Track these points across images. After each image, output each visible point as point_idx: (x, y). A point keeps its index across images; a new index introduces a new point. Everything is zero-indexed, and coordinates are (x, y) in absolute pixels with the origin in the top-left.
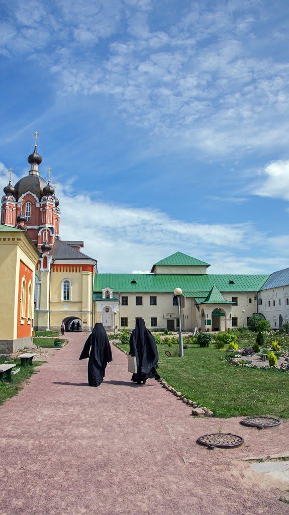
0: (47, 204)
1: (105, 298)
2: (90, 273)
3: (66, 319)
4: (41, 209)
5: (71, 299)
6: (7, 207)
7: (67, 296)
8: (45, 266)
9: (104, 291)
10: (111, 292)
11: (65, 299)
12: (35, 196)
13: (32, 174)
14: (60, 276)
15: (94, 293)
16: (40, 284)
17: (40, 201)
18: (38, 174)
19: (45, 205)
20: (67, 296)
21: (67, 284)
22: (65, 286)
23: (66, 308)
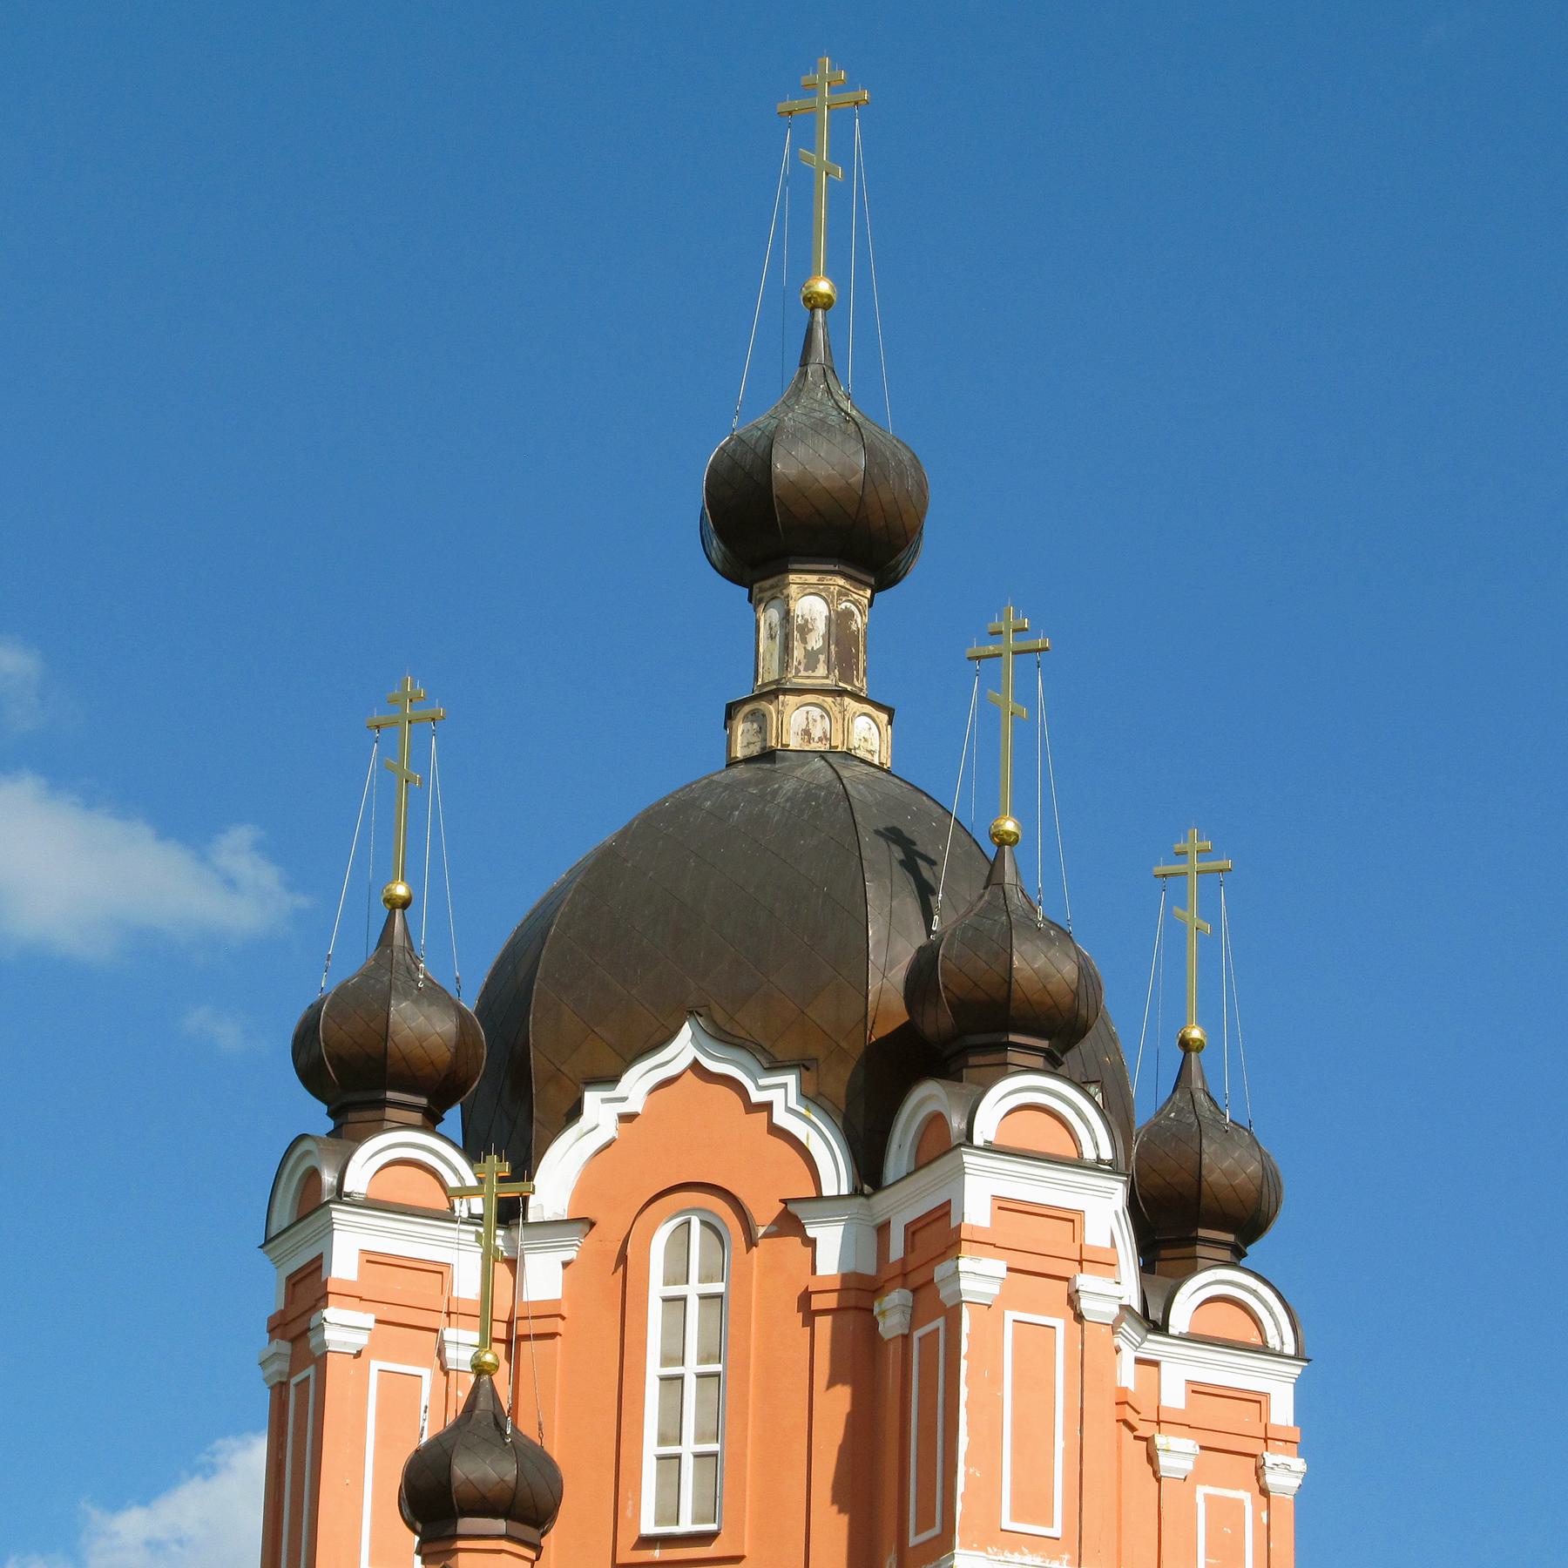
0: (976, 1212)
4: (892, 1313)
6: (343, 1327)
12: (781, 1093)
13: (768, 755)
17: (868, 1171)
18: (867, 734)
19: (939, 1234)
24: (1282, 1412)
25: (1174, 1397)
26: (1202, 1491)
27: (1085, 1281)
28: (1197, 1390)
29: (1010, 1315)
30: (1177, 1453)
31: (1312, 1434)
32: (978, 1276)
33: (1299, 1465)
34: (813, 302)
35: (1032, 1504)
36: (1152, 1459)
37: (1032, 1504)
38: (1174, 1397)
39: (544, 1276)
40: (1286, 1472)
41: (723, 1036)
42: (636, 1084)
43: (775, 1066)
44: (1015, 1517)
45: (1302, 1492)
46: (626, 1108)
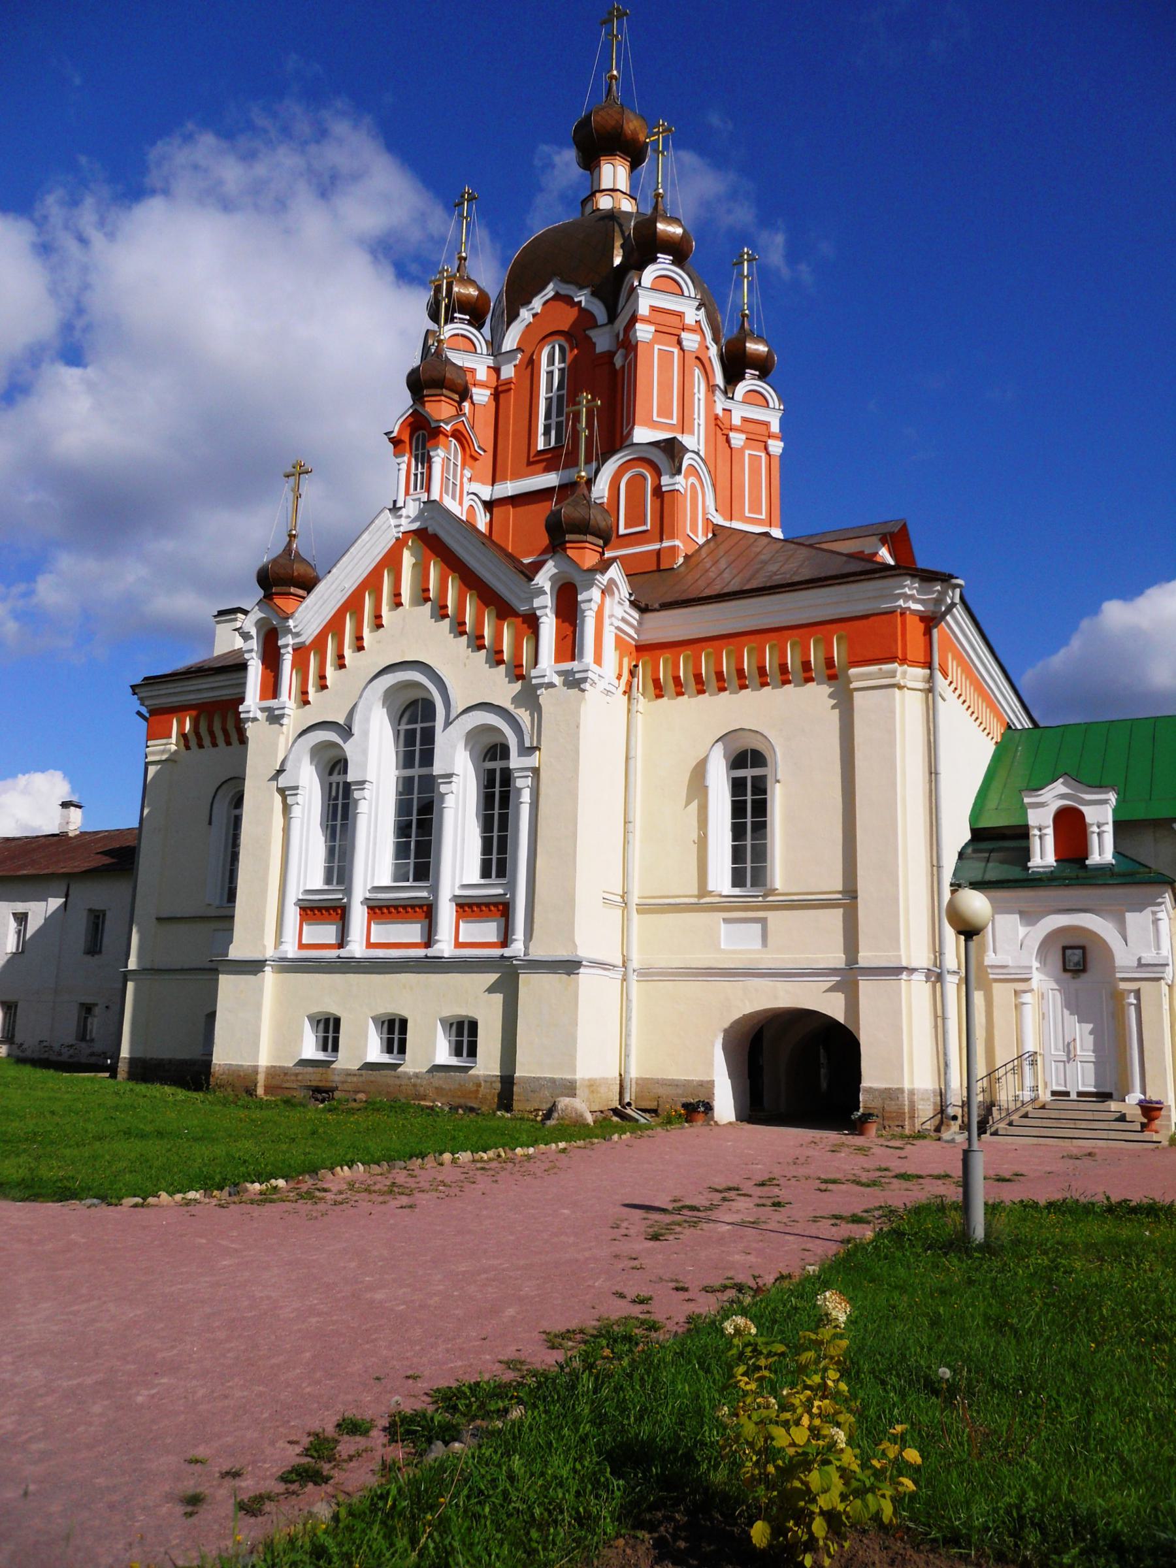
1: (1050, 859)
2: (914, 675)
3: (737, 1022)
4: (618, 361)
5: (782, 870)
7: (750, 859)
8: (569, 647)
9: (1041, 818)
10: (1100, 815)
11: (738, 879)
14: (700, 724)
15: (979, 835)
16: (536, 771)
20: (750, 859)
21: (748, 773)
22: (738, 786)
23: (736, 941)
24: (775, 428)
25: (736, 421)
26: (747, 452)
27: (684, 335)
28: (745, 420)
29: (656, 347)
30: (737, 439)
31: (784, 435)
32: (644, 332)
33: (782, 444)
34: (613, 77)
35: (665, 411)
36: (728, 441)
37: (665, 411)
38: (736, 421)
39: (508, 372)
40: (776, 447)
41: (565, 280)
42: (537, 304)
43: (581, 288)
44: (658, 416)
45: (781, 456)
46: (534, 312)
